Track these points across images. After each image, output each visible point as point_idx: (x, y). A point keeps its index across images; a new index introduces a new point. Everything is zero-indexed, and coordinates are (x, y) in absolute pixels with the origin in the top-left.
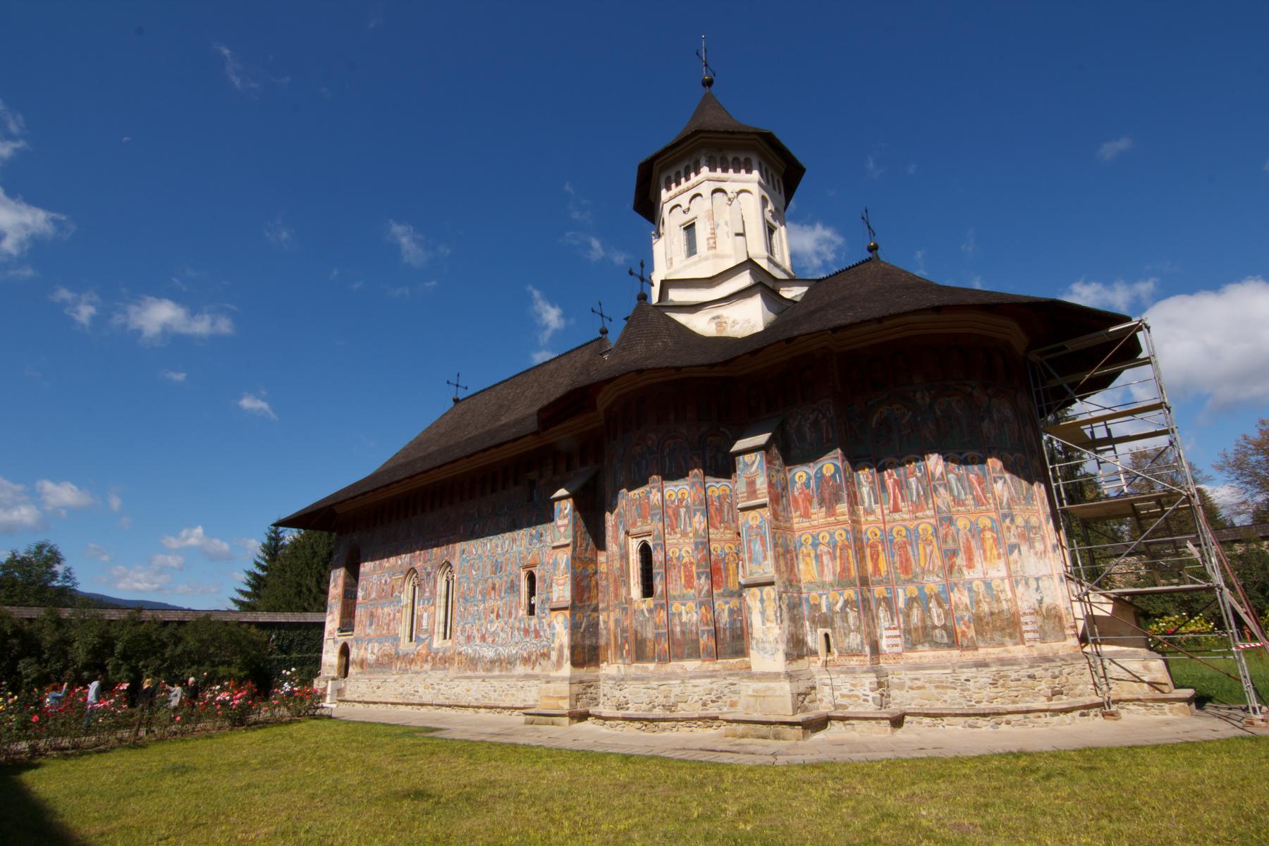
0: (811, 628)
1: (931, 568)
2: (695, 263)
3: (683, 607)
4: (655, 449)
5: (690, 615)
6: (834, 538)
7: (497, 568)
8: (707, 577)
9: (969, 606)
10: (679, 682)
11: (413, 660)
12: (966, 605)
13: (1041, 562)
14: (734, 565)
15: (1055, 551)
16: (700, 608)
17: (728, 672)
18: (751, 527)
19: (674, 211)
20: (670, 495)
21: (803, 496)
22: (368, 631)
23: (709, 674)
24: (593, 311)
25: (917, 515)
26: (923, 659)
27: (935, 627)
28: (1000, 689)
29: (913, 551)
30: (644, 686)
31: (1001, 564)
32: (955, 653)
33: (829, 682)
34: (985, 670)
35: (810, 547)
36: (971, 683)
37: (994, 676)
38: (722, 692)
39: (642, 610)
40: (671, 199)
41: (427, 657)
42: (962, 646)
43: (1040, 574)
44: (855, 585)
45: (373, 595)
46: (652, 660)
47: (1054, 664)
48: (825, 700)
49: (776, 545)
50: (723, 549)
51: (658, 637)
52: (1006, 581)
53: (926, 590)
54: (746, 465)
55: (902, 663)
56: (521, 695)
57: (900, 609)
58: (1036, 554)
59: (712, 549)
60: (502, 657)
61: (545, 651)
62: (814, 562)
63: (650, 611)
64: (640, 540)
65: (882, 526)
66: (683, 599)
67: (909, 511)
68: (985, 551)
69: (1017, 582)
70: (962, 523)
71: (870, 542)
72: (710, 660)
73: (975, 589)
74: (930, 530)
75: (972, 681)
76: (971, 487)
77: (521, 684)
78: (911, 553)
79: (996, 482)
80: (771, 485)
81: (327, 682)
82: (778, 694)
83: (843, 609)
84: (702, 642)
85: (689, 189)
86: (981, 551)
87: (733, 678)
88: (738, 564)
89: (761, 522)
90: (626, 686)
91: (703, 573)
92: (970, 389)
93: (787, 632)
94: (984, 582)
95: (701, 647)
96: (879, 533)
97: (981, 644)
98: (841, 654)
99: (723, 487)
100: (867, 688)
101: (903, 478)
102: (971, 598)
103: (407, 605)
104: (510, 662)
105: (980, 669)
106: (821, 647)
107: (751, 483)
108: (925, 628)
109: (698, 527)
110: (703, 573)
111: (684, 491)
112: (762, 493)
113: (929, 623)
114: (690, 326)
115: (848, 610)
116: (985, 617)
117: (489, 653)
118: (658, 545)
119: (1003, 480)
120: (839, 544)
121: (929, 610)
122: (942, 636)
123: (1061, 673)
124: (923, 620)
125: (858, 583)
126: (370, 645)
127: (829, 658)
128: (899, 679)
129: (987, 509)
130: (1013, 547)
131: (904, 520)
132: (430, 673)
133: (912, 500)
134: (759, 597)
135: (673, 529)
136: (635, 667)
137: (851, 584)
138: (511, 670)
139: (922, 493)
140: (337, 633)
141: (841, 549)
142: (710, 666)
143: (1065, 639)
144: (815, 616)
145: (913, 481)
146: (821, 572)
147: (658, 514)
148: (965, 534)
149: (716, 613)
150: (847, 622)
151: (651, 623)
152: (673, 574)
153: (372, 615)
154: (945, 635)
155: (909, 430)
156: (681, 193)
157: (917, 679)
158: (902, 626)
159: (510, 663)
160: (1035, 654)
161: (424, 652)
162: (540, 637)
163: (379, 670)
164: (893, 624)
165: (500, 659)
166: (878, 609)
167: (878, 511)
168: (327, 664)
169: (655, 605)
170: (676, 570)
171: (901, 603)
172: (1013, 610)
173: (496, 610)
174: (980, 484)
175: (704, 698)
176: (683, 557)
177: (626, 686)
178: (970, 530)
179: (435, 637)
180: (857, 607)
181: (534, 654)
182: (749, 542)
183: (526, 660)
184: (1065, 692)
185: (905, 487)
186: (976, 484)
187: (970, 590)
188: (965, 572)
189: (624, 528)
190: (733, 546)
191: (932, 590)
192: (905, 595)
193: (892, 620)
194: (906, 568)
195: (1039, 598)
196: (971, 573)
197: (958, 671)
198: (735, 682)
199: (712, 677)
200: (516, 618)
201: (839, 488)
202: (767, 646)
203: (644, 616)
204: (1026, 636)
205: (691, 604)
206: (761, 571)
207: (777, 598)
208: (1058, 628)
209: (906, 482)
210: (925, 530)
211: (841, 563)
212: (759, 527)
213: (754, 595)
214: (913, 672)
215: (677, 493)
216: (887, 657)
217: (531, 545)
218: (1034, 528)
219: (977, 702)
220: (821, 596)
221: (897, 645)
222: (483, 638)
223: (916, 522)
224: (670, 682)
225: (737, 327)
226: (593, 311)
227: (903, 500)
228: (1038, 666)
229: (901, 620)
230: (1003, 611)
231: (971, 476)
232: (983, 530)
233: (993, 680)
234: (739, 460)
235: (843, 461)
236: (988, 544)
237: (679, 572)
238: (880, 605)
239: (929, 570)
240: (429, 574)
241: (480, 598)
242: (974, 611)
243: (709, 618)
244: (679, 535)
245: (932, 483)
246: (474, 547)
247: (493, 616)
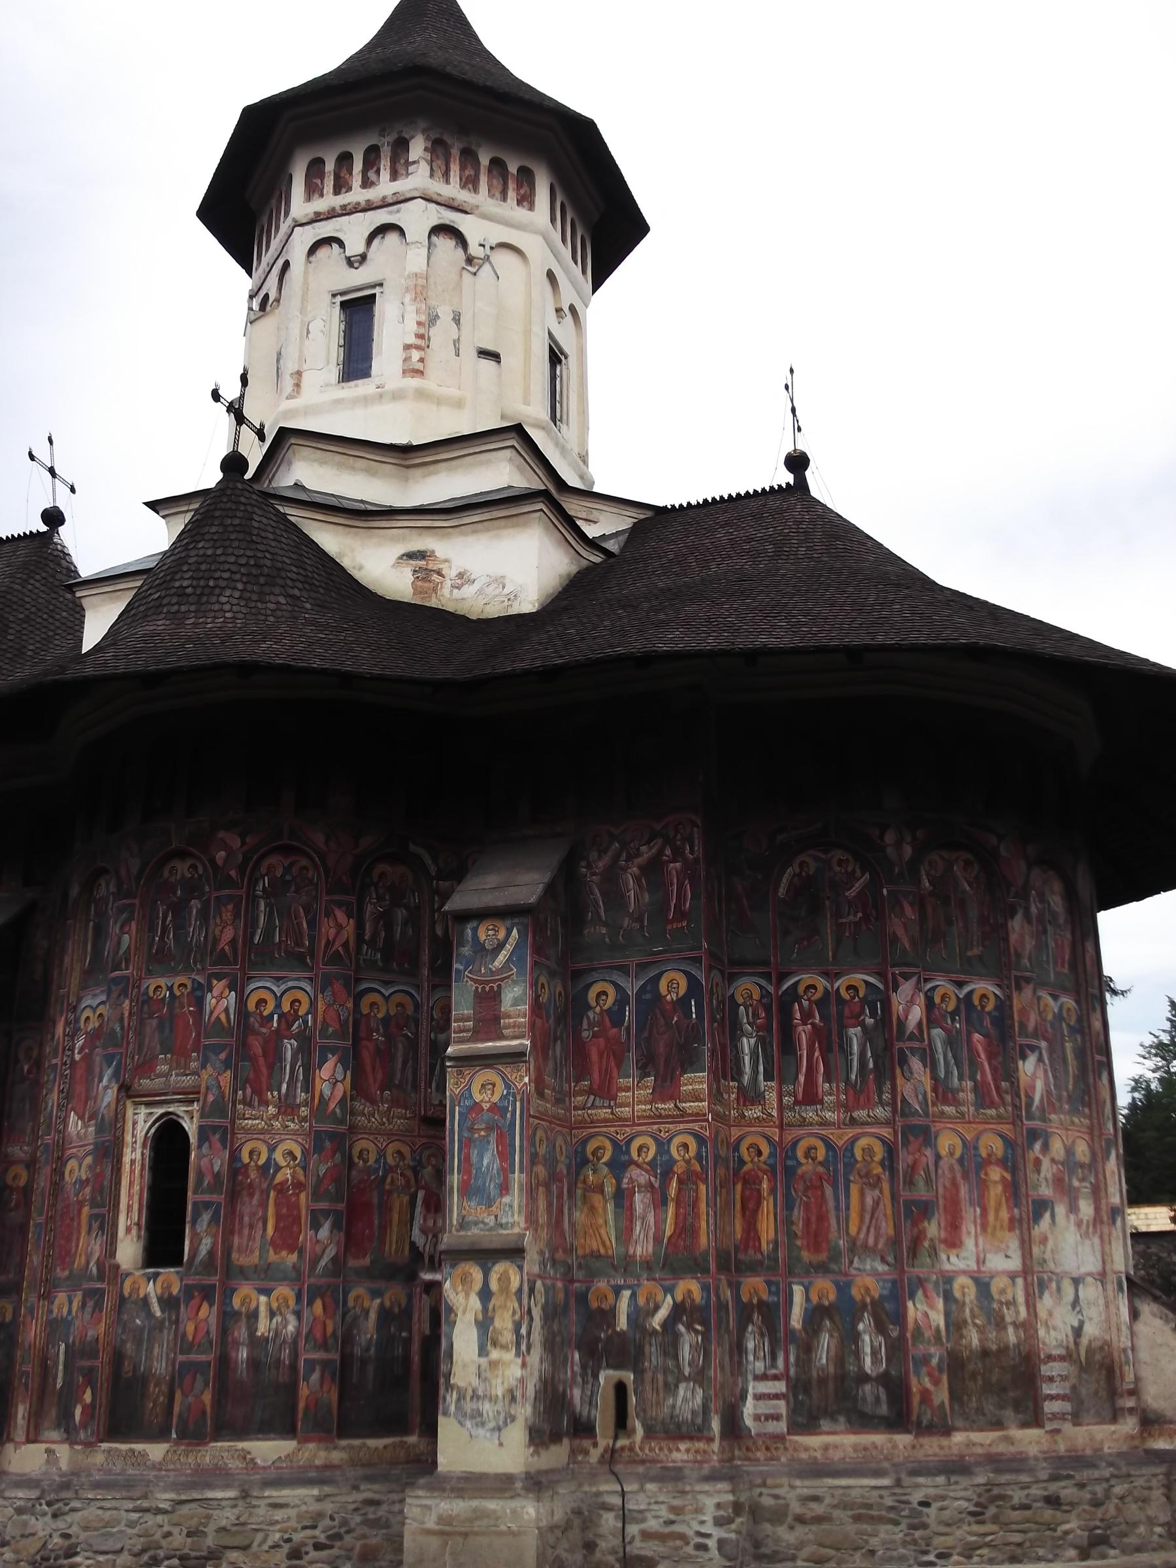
0: (584, 1367)
1: (871, 1241)
2: (366, 401)
3: (263, 1299)
4: (233, 873)
5: (279, 1319)
6: (668, 1151)
8: (336, 1226)
9: (943, 1333)
10: (231, 1494)
12: (938, 1330)
13: (1088, 1242)
14: (406, 1199)
16: (310, 1303)
17: (360, 1472)
18: (477, 1106)
19: (323, 252)
20: (262, 1002)
21: (602, 1041)
23: (312, 1474)
24: (32, 457)
25: (855, 1114)
26: (831, 1452)
27: (863, 1378)
28: (989, 1528)
29: (837, 1199)
30: (130, 1505)
31: (1014, 1244)
32: (903, 1440)
33: (616, 1500)
34: (964, 1481)
35: (606, 1170)
36: (932, 1511)
37: (980, 1495)
38: (345, 1522)
39: (146, 1300)
40: (318, 218)
42: (919, 1423)
43: (1083, 1270)
44: (706, 1271)
46: (161, 1435)
47: (1096, 1474)
48: (603, 1545)
49: (534, 1159)
50: (382, 1153)
51: (182, 1375)
52: (1020, 1281)
53: (855, 1292)
54: (479, 948)
55: (783, 1459)
57: (793, 1331)
58: (1079, 1224)
59: (355, 1153)
62: (610, 1207)
63: (169, 1303)
64: (160, 1111)
65: (775, 1133)
66: (265, 1277)
67: (838, 1105)
69: (1042, 1285)
70: (947, 1142)
71: (745, 1168)
72: (320, 1440)
73: (957, 1294)
74: (879, 1152)
75: (936, 1505)
76: (974, 1064)
78: (831, 1204)
79: (1024, 1057)
80: (537, 1008)
82: (503, 1528)
83: (670, 1323)
84: (304, 1391)
85: (369, 207)
86: (978, 1210)
87: (376, 1487)
88: (414, 1198)
89: (503, 1098)
90: (76, 1504)
91: (326, 1213)
92: (994, 841)
93: (536, 1374)
94: (976, 1281)
95: (301, 1405)
96: (766, 1150)
97: (959, 1423)
98: (650, 1433)
99: (399, 998)
100: (708, 1518)
101: (834, 1027)
102: (947, 1315)
105: (953, 1479)
106: (602, 1417)
107: (489, 999)
108: (842, 1377)
109: (327, 1092)
110: (326, 1213)
111: (300, 995)
112: (519, 1026)
113: (852, 1368)
114: (346, 563)
115: (681, 1328)
116: (969, 1359)
118: (215, 1129)
119: (1037, 1054)
120: (679, 1168)
121: (856, 1337)
122: (878, 1399)
123: (1108, 1494)
124: (840, 1361)
125: (713, 1266)
127: (620, 1443)
128: (776, 1497)
129: (999, 1116)
130: (1041, 1207)
131: (824, 1123)
133: (847, 1081)
134: (478, 1284)
135: (258, 1092)
136: (109, 1451)
137: (695, 1266)
139: (871, 1065)
141: (680, 1181)
142: (315, 1453)
143: (1114, 1419)
144: (598, 1339)
145: (854, 1032)
146: (625, 1234)
147: (222, 1048)
148: (951, 1169)
149: (348, 1318)
150: (676, 1357)
151: (167, 1336)
152: (247, 1210)
154: (883, 1397)
155: (860, 915)
156: (347, 211)
157: (816, 1499)
158: (792, 1371)
160: (1062, 1448)
164: (774, 1365)
166: (742, 1331)
167: (772, 1097)
169: (188, 1291)
170: (255, 1201)
171: (796, 1319)
172: (1024, 1349)
174: (991, 1057)
175: (297, 1537)
176: (278, 1168)
177: (76, 1504)
178: (961, 1161)
180: (703, 1323)
182: (466, 1144)
184: (1113, 1539)
185: (836, 1047)
186: (983, 1056)
187: (948, 1297)
188: (943, 1257)
189: (116, 1075)
190: (406, 1150)
191: (867, 1290)
192: (808, 1299)
193: (774, 1357)
194: (817, 1237)
195: (1076, 1324)
196: (953, 1259)
197: (907, 1481)
198: (376, 1497)
199: (320, 1482)
201: (694, 1034)
202: (487, 1407)
203: (150, 1314)
204: (1050, 1407)
205: (284, 1291)
206: (490, 1220)
207: (526, 1288)
208: (1103, 1394)
209: (841, 1035)
210: (869, 1151)
211: (677, 1215)
212: (494, 1108)
213: (465, 1280)
214: (807, 1483)
215: (279, 1000)
216: (750, 1444)
218: (1082, 1166)
219: (940, 1556)
220: (617, 1291)
221: (776, 1417)
223: (850, 1132)
224: (210, 1494)
225: (468, 591)
226: (32, 457)
227: (828, 1078)
228: (1069, 1477)
229: (792, 1359)
230: (1007, 1348)
231: (977, 1036)
232: (987, 1162)
233: (977, 1505)
234: (462, 933)
235: (710, 968)
236: (992, 1193)
237: (264, 1205)
238: (750, 1320)
239: (865, 1246)
242: (949, 1346)
243: (330, 1330)
244: (272, 1110)
245: (898, 1045)
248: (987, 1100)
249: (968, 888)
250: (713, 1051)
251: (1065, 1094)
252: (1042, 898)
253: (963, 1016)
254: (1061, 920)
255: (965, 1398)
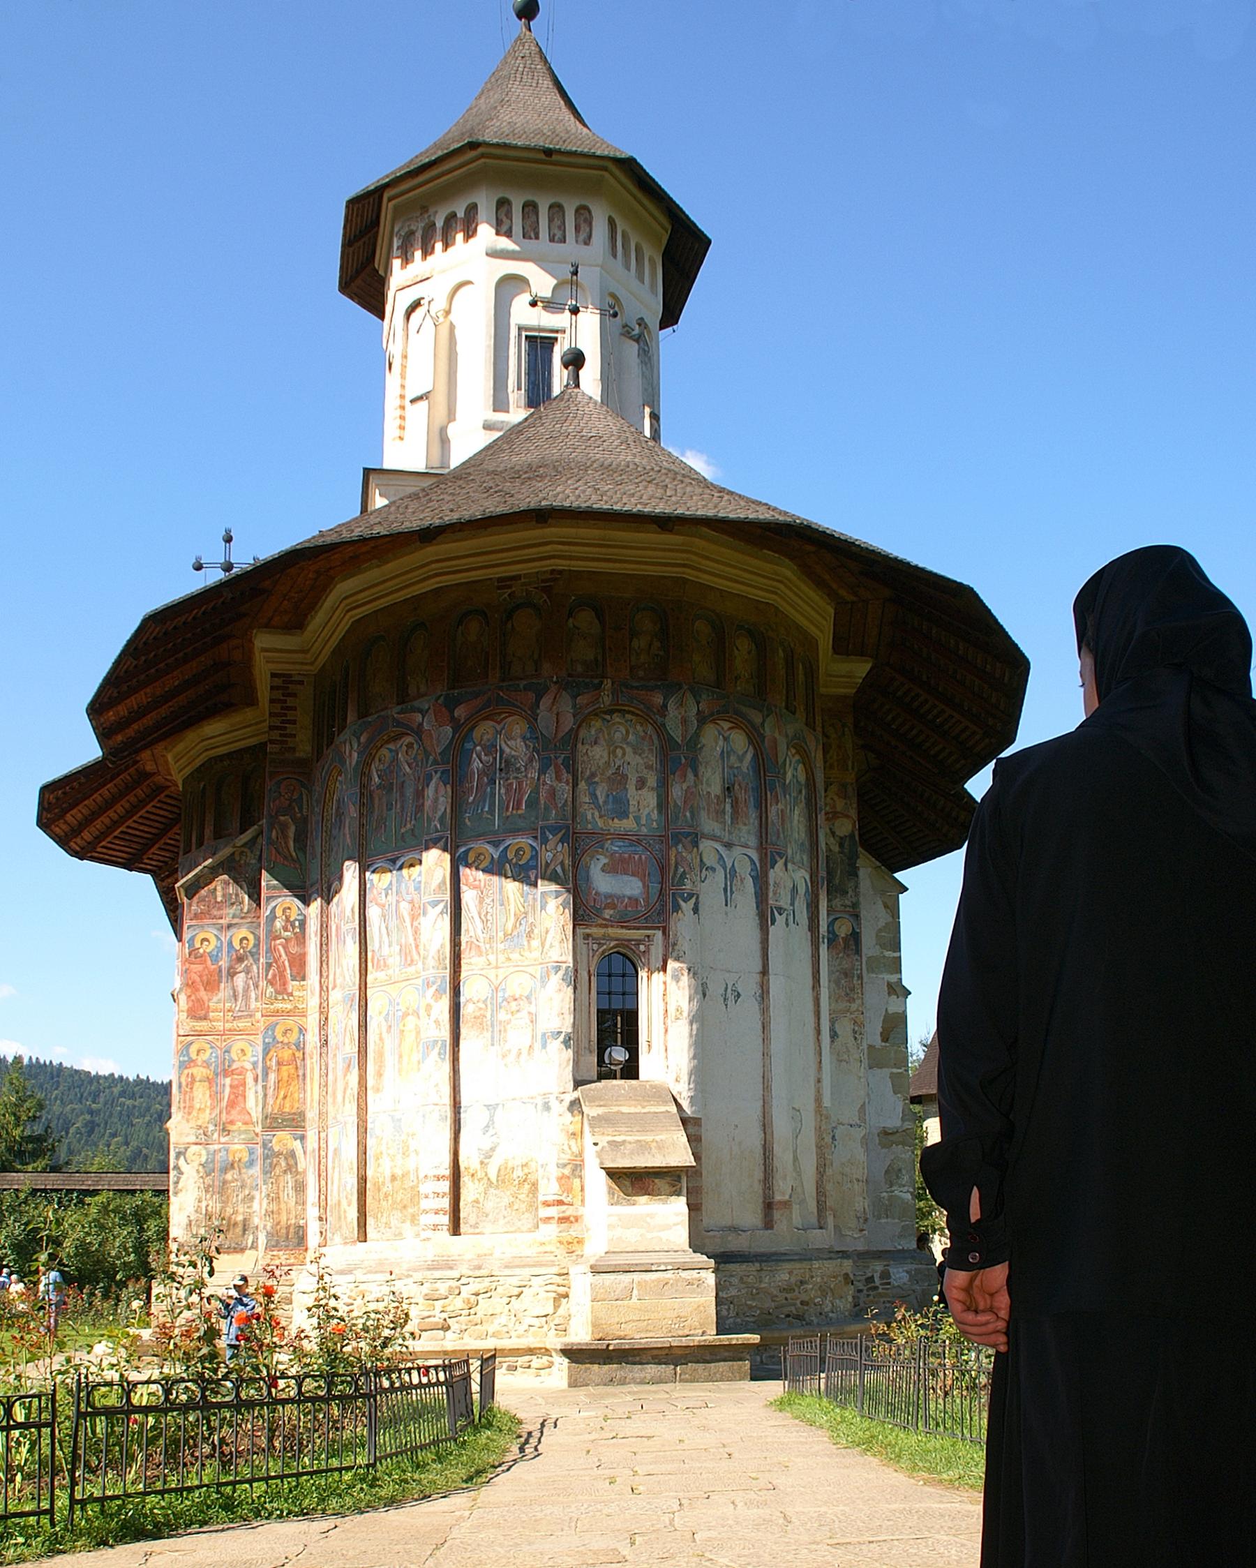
15: (544, 1046)
37: (351, 1291)
47: (438, 1274)
68: (400, 1056)
79: (425, 914)
86: (397, 1057)
92: (419, 717)
119: (441, 906)
148: (379, 1026)
195: (487, 1147)
228: (409, 1276)
248: (409, 959)
249: (408, 769)
250: (269, 966)
251: (501, 934)
252: (490, 748)
253: (394, 889)
254: (521, 763)
255: (379, 1215)
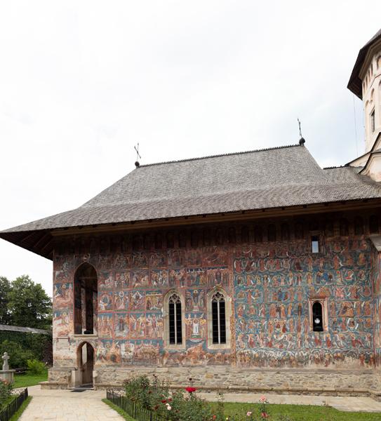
7: (280, 296)
11: (183, 357)
22: (118, 334)
41: (202, 355)
45: (122, 307)
56: (321, 383)
60: (292, 358)
61: (339, 354)
77: (321, 376)
81: (71, 372)
103: (165, 317)
104: (302, 361)
117: (276, 354)
126: (123, 346)
132: (207, 367)
138: (302, 366)
140: (71, 334)
153: (121, 322)
159: (302, 362)
161: (197, 352)
162: (333, 345)
163: (138, 363)
165: (290, 359)
168: (62, 357)
173: (282, 326)
179: (208, 341)
181: (327, 357)
183: (317, 361)
200: (304, 332)
217: (319, 283)
222: (269, 344)
240: (196, 296)
241: (263, 316)
246: (251, 279)
247: (280, 330)
